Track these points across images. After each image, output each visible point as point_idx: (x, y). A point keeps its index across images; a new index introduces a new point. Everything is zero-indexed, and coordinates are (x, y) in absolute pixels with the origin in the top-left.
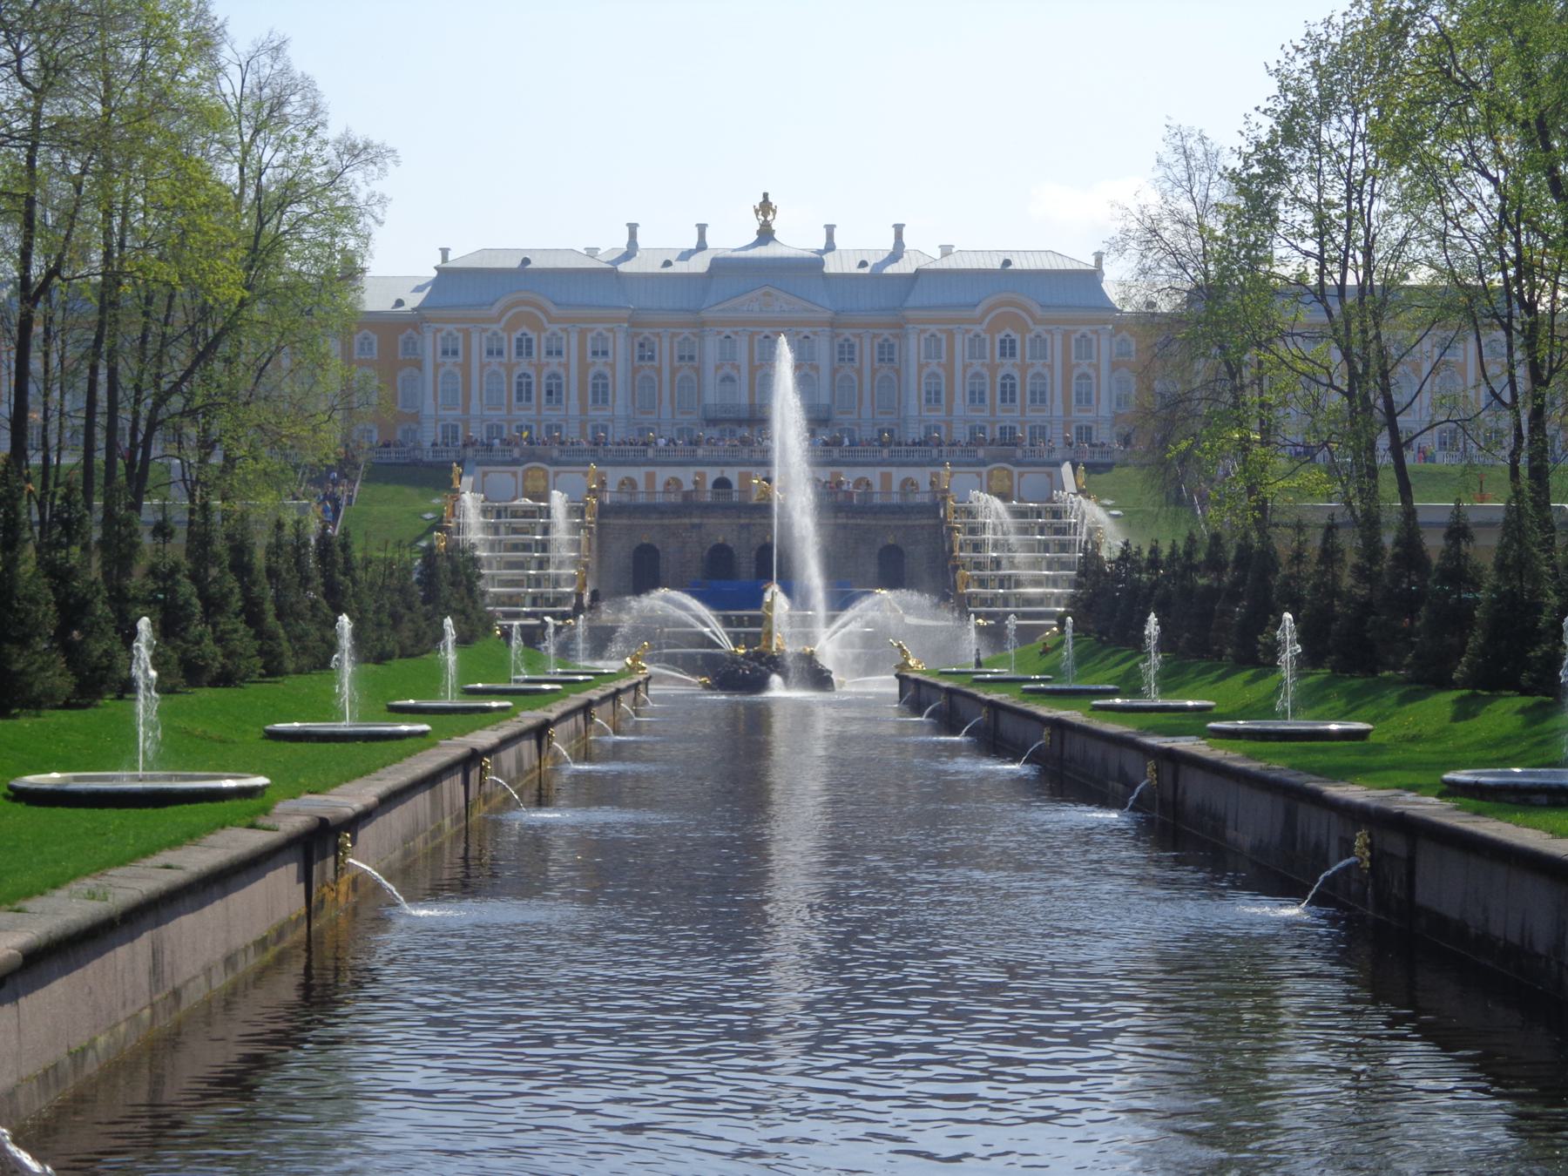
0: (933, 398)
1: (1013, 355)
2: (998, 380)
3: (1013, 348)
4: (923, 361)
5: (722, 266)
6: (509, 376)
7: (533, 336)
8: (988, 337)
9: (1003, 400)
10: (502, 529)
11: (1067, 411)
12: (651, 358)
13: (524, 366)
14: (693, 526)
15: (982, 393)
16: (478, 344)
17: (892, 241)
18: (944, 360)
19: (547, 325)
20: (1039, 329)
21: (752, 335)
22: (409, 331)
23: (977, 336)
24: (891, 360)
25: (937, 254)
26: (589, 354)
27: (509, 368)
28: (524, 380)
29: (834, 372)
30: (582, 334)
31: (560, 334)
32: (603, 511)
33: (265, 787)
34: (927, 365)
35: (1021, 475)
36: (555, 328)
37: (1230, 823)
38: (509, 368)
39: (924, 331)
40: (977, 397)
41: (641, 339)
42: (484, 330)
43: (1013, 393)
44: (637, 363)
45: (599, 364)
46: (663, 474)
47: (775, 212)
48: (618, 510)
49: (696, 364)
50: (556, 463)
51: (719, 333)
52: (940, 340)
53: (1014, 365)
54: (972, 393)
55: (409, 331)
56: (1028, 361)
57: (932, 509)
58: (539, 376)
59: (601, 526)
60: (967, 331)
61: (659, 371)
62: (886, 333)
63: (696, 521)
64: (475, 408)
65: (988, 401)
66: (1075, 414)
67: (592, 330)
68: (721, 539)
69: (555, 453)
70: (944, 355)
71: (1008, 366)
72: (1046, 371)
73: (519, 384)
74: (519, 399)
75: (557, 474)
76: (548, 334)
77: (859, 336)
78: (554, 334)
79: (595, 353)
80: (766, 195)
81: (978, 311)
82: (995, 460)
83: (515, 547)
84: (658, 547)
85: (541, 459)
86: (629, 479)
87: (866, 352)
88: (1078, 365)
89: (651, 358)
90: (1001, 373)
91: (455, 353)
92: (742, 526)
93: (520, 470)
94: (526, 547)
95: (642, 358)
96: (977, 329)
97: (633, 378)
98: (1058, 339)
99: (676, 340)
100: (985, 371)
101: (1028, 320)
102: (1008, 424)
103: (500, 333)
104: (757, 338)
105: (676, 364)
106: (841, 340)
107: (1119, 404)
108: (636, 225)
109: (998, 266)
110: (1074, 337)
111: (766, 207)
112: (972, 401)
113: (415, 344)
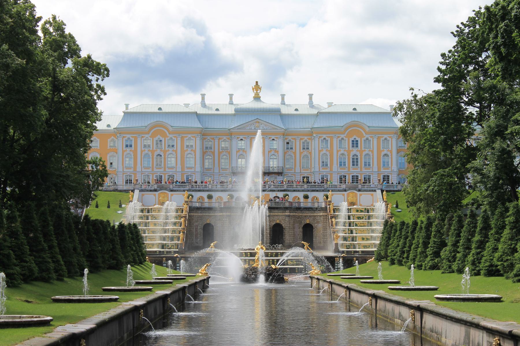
0: (324, 164)
1: (357, 146)
2: (351, 156)
4: (320, 149)
5: (240, 112)
6: (153, 155)
9: (353, 165)
10: (150, 217)
17: (229, 100)
18: (329, 149)
19: (168, 135)
20: (367, 136)
22: (113, 137)
24: (308, 148)
25: (326, 106)
27: (153, 152)
32: (192, 209)
33: (51, 320)
34: (322, 150)
35: (360, 195)
36: (171, 136)
37: (443, 336)
38: (153, 152)
39: (320, 137)
43: (357, 162)
44: (205, 150)
47: (260, 89)
48: (198, 209)
50: (172, 191)
52: (328, 140)
54: (340, 162)
55: (113, 137)
56: (363, 149)
57: (325, 209)
59: (189, 216)
60: (338, 137)
61: (214, 153)
64: (139, 169)
69: (171, 187)
71: (355, 151)
72: (370, 153)
75: (172, 195)
78: (171, 138)
80: (257, 82)
82: (350, 189)
85: (166, 189)
86: (201, 197)
88: (383, 151)
90: (352, 154)
91: (131, 146)
93: (157, 193)
99: (220, 141)
100: (346, 153)
102: (355, 174)
108: (205, 94)
110: (382, 139)
112: (341, 165)
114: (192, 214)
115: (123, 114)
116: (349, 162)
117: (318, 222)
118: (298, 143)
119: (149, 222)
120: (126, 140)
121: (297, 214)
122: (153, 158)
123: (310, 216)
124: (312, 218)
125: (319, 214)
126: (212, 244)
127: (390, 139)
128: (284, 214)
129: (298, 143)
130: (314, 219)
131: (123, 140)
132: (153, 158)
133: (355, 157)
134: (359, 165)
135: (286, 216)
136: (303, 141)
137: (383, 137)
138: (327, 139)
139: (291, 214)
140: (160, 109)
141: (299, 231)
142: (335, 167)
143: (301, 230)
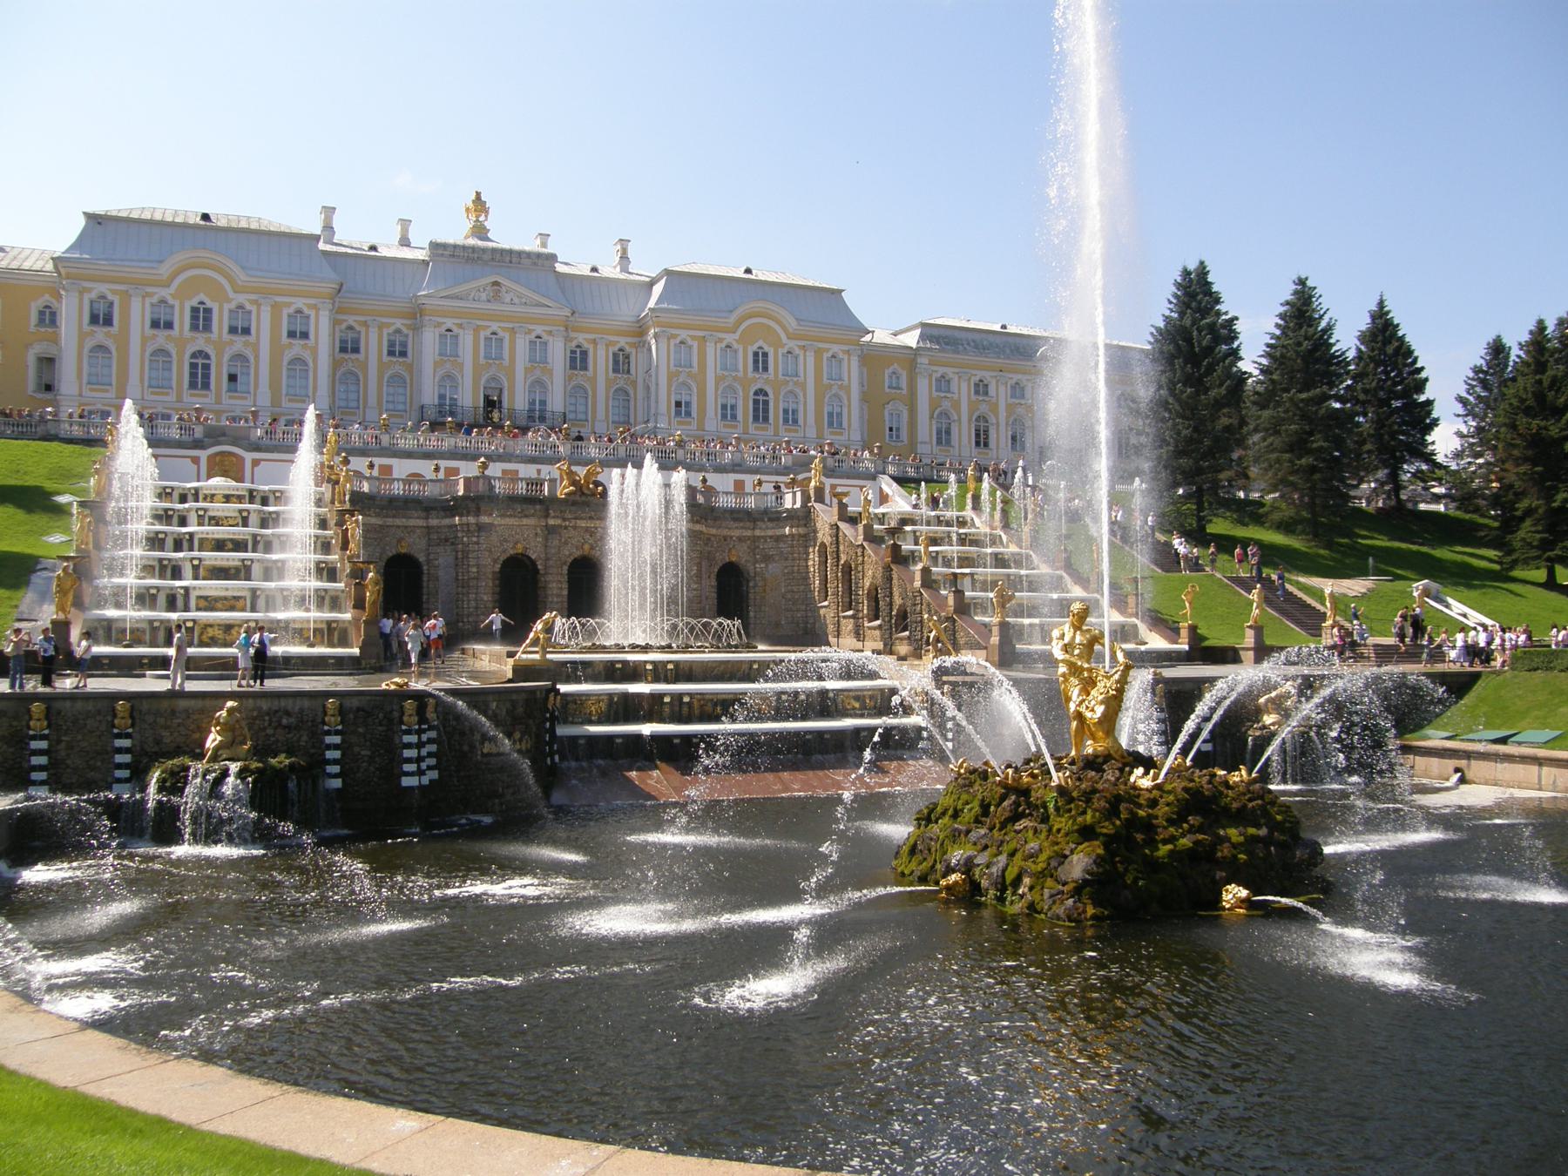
1: (766, 369)
3: (765, 363)
7: (215, 307)
9: (756, 418)
11: (820, 436)
12: (356, 350)
13: (200, 342)
14: (481, 527)
15: (733, 407)
16: (138, 315)
18: (695, 369)
19: (231, 295)
20: (791, 344)
26: (285, 334)
28: (200, 361)
29: (570, 379)
30: (276, 308)
31: (248, 307)
36: (242, 298)
40: (728, 413)
41: (344, 326)
43: (766, 411)
46: (402, 468)
47: (486, 212)
49: (409, 360)
50: (257, 448)
51: (439, 325)
52: (690, 347)
54: (724, 407)
55: (47, 296)
58: (220, 355)
60: (721, 340)
61: (365, 366)
62: (623, 342)
63: (485, 519)
65: (740, 417)
66: (826, 431)
67: (289, 305)
68: (520, 549)
70: (695, 364)
73: (193, 366)
74: (193, 385)
75: (256, 463)
76: (233, 305)
77: (594, 342)
78: (241, 307)
79: (291, 334)
80: (478, 194)
81: (733, 318)
83: (220, 545)
84: (422, 559)
87: (601, 361)
89: (356, 350)
92: (550, 530)
93: (204, 455)
94: (239, 546)
95: (343, 350)
96: (729, 338)
97: (334, 374)
99: (385, 332)
101: (783, 336)
103: (171, 301)
104: (483, 334)
105: (386, 358)
106: (574, 344)
110: (826, 355)
111: (479, 204)
112: (724, 417)
113: (53, 314)
116: (744, 409)
117: (767, 559)
118: (601, 352)
119: (191, 535)
120: (92, 302)
122: (180, 361)
123: (740, 539)
124: (744, 547)
125: (770, 533)
126: (539, 626)
129: (601, 352)
130: (753, 550)
131: (81, 300)
132: (180, 361)
134: (771, 420)
138: (690, 342)
140: (206, 217)
142: (713, 423)
143: (714, 583)
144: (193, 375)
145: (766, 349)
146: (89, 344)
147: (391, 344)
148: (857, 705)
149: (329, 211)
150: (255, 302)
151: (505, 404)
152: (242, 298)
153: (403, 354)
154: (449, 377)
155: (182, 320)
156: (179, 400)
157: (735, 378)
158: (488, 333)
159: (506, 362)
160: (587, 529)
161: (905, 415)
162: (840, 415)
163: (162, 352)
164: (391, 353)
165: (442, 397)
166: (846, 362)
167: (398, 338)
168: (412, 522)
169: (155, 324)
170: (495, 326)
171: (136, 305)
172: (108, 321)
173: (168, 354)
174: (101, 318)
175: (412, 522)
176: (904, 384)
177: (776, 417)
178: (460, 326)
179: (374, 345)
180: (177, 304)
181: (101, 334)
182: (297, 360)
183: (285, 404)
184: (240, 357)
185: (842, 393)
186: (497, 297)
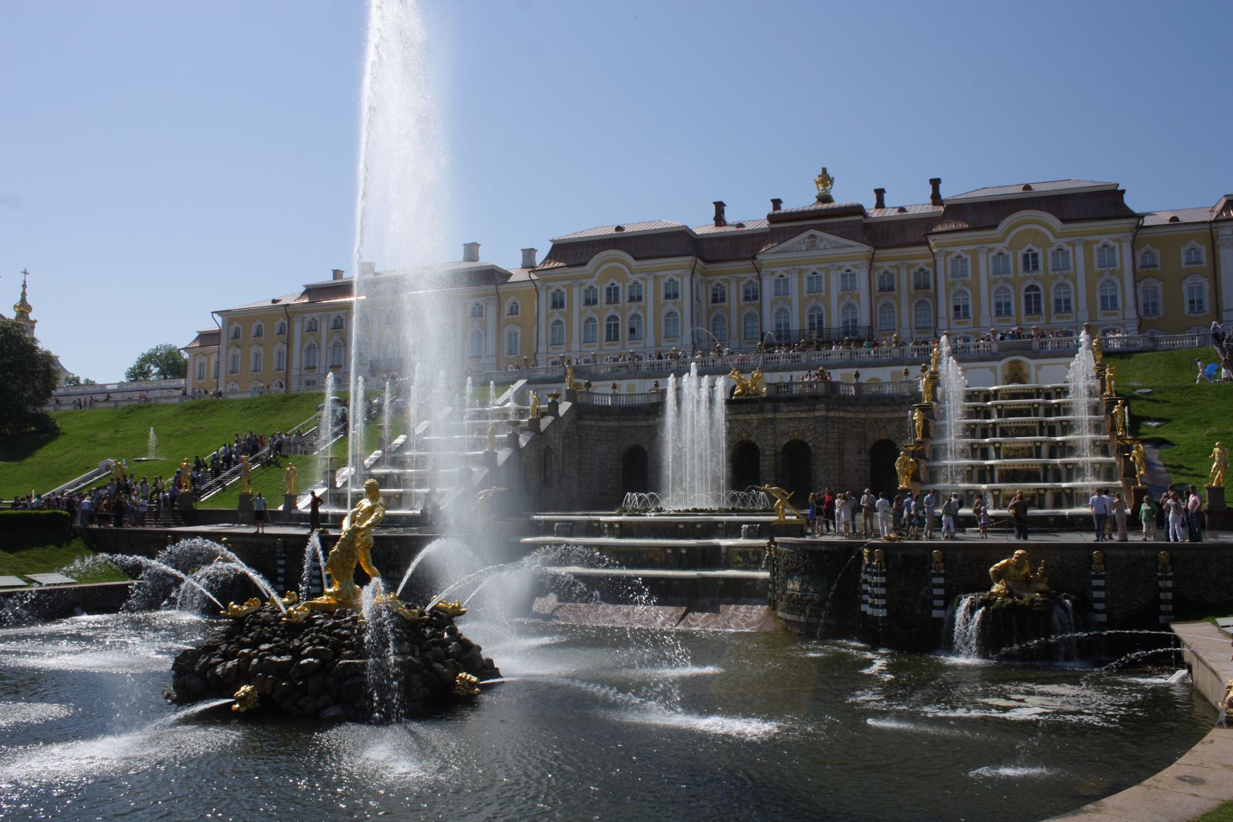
1: (1036, 267)
2: (1023, 290)
8: (1011, 254)
9: (1028, 311)
12: (723, 300)
13: (611, 310)
15: (1008, 305)
16: (576, 299)
18: (970, 278)
19: (630, 276)
20: (1059, 242)
21: (801, 272)
23: (1001, 254)
26: (662, 295)
31: (640, 282)
35: (1038, 367)
36: (634, 278)
40: (1002, 309)
41: (713, 284)
42: (581, 284)
43: (1038, 303)
45: (670, 305)
47: (832, 181)
48: (604, 412)
49: (758, 302)
51: (773, 273)
53: (1036, 278)
54: (998, 305)
56: (1051, 272)
60: (990, 250)
64: (575, 346)
65: (1013, 312)
67: (664, 276)
70: (970, 273)
73: (609, 326)
76: (630, 283)
77: (896, 267)
79: (668, 296)
80: (824, 170)
89: (723, 300)
95: (715, 301)
96: (999, 247)
98: (1080, 252)
99: (742, 284)
104: (805, 275)
105: (742, 303)
106: (881, 271)
107: (1146, 312)
109: (1019, 190)
110: (1096, 247)
112: (999, 313)
114: (584, 422)
115: (550, 245)
116: (1018, 302)
118: (904, 274)
121: (850, 415)
123: (890, 420)
127: (1117, 245)
128: (811, 415)
129: (904, 274)
133: (1032, 293)
135: (815, 417)
136: (916, 269)
137: (1097, 242)
138: (964, 256)
139: (832, 414)
141: (857, 460)
144: (609, 332)
145: (1036, 250)
146: (550, 323)
147: (747, 292)
148: (741, 559)
149: (720, 206)
150: (642, 279)
151: (824, 326)
152: (634, 278)
153: (755, 298)
154: (782, 310)
155: (602, 297)
156: (601, 349)
157: (1006, 280)
158: (809, 273)
159: (823, 294)
160: (745, 421)
161: (1207, 287)
162: (1114, 298)
163: (591, 319)
164: (747, 298)
165: (778, 325)
166: (1117, 249)
167: (750, 287)
168: (639, 424)
169: (588, 303)
170: (813, 268)
171: (576, 292)
172: (562, 306)
173: (594, 320)
174: (557, 304)
175: (639, 424)
176: (1204, 257)
177: (1048, 306)
178: (787, 272)
179: (734, 294)
180: (598, 287)
181: (557, 314)
182: (671, 314)
183: (664, 343)
184: (635, 317)
185: (1114, 278)
186: (813, 245)
